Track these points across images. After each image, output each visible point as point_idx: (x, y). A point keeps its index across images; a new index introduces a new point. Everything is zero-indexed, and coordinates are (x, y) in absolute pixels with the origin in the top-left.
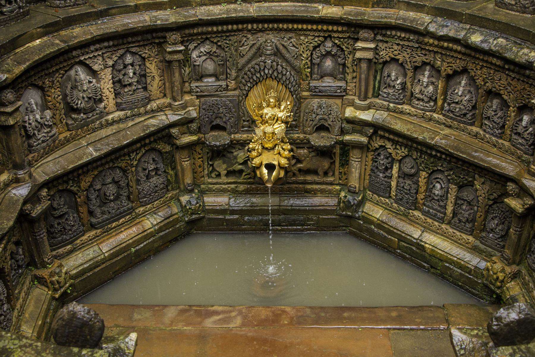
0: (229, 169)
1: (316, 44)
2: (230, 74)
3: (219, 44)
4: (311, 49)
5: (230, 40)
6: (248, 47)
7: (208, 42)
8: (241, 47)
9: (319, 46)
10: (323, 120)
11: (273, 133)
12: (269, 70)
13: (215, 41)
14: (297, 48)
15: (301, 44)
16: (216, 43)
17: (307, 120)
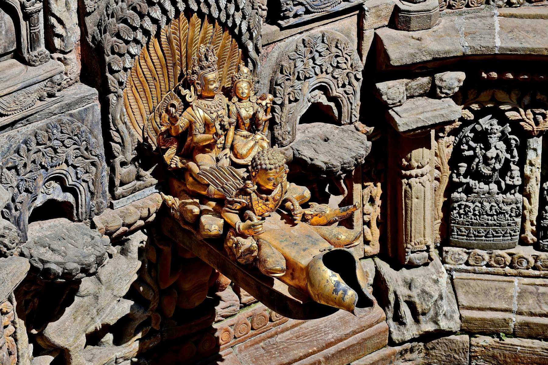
0: (91, 329)
2: (60, 36)
10: (317, 92)
17: (282, 105)
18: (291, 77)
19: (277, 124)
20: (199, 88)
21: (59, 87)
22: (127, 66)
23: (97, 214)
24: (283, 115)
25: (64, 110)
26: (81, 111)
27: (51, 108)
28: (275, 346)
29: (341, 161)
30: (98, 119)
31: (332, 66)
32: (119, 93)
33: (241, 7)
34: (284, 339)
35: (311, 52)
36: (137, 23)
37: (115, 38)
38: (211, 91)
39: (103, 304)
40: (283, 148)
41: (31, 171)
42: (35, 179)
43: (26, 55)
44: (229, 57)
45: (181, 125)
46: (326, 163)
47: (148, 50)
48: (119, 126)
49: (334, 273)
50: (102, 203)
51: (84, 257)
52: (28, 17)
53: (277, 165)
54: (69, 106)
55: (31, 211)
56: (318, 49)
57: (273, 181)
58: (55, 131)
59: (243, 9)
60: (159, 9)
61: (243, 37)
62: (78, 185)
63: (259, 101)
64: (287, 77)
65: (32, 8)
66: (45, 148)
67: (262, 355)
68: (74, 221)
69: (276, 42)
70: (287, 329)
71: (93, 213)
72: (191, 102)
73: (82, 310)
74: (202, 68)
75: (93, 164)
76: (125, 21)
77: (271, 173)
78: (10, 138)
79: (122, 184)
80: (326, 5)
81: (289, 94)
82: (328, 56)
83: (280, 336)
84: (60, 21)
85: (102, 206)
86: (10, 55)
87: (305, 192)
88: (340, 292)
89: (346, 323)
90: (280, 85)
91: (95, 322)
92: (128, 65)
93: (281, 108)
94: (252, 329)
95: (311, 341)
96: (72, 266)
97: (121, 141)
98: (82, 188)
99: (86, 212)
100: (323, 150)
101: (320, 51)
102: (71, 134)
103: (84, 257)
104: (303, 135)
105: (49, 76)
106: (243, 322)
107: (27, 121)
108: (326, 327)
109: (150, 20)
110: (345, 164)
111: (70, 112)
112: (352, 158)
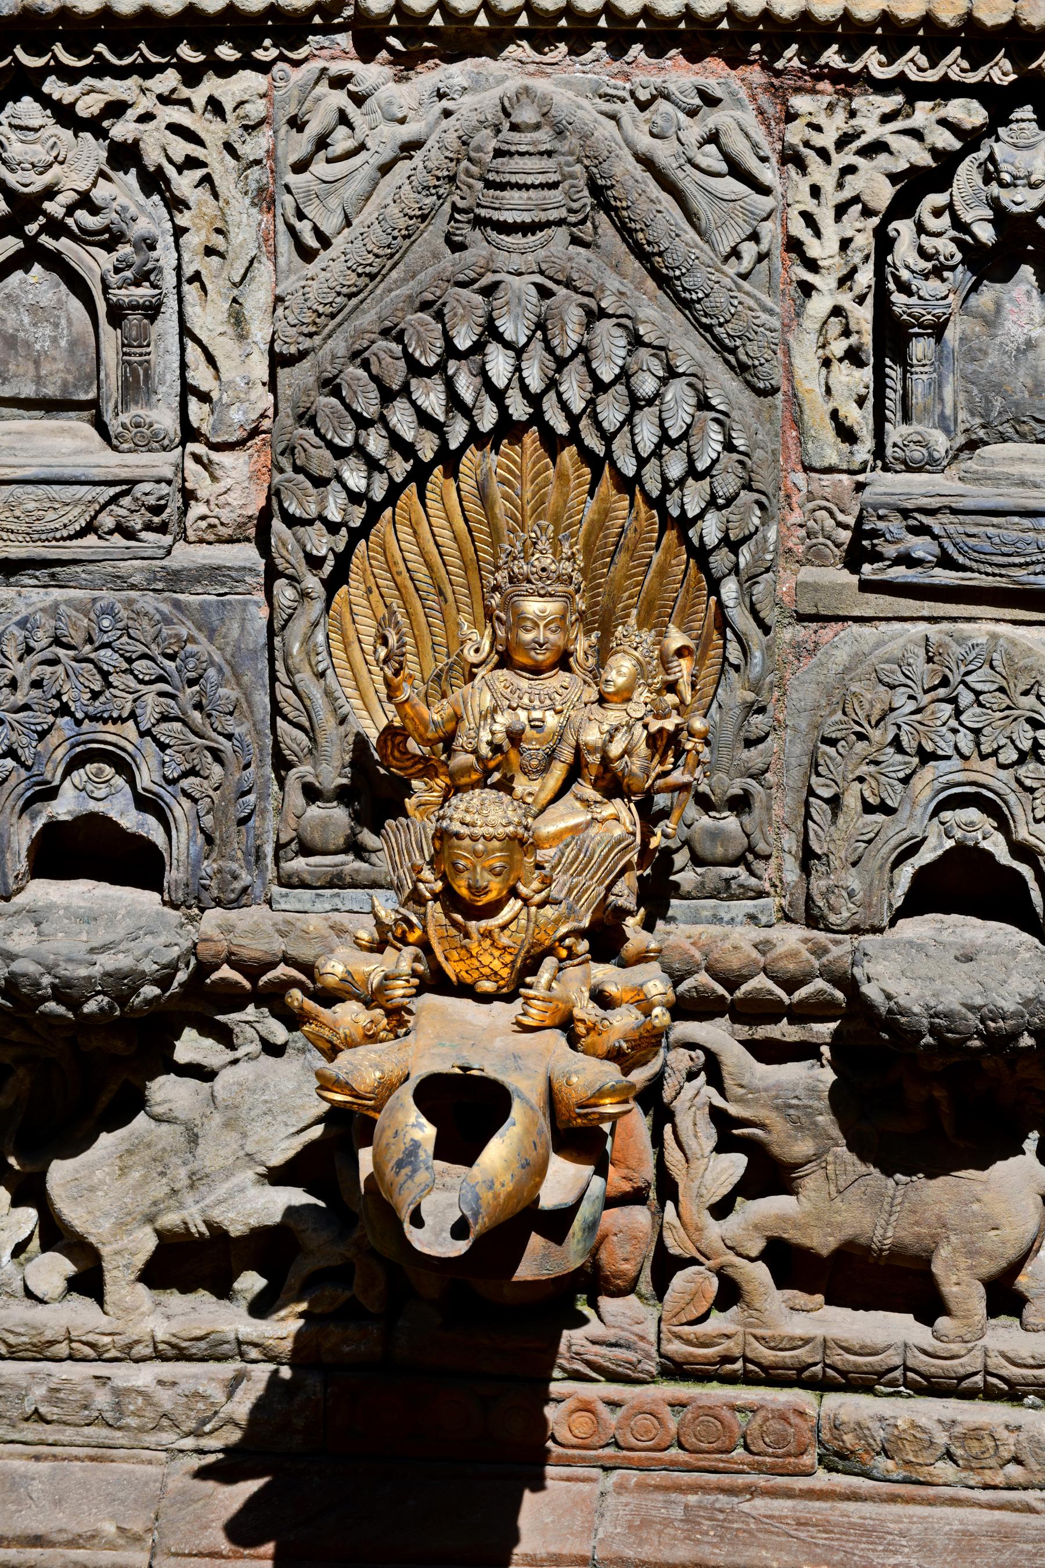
0: (170, 1220)
1: (912, 154)
2: (205, 397)
3: (122, 130)
4: (883, 194)
5: (215, 106)
6: (365, 164)
7: (27, 109)
8: (300, 167)
9: (939, 173)
10: (972, 814)
11: (520, 843)
12: (520, 352)
13: (88, 106)
14: (764, 190)
15: (792, 158)
16: (94, 126)
17: (835, 802)
18: (875, 735)
19: (818, 857)
20: (501, 633)
21: (156, 520)
22: (330, 517)
23: (219, 903)
24: (835, 836)
25: (160, 585)
26: (210, 604)
27: (122, 564)
28: (721, 1516)
29: (932, 1003)
30: (256, 642)
31: (1016, 748)
32: (303, 585)
33: (701, 466)
34: (762, 1512)
35: (945, 682)
36: (368, 404)
37: (309, 433)
38: (526, 648)
39: (207, 1163)
41: (26, 707)
42: (42, 735)
43: (108, 417)
45: (436, 717)
46: (889, 997)
47: (424, 506)
48: (298, 677)
49: (423, 1120)
50: (235, 877)
51: (70, 960)
52: (117, 315)
53: (478, 831)
54: (176, 580)
56: (968, 679)
57: (466, 874)
58: (106, 623)
59: (707, 472)
60: (442, 388)
61: (712, 559)
62: (168, 798)
63: (649, 719)
64: (858, 729)
65: (123, 291)
67: (667, 1522)
68: (165, 903)
69: (844, 619)
70: (788, 1494)
71: (205, 896)
72: (477, 666)
73: (147, 1154)
74: (512, 579)
75: (217, 755)
76: (331, 386)
77: (459, 848)
79: (306, 850)
80: (1011, 560)
81: (861, 779)
83: (758, 1502)
84: (211, 360)
85: (238, 885)
86: (86, 414)
87: (650, 984)
88: (407, 1170)
89: (972, 1550)
90: (832, 742)
91: (181, 1206)
92: (334, 515)
93: (835, 815)
94: (681, 1446)
95: (831, 1548)
96: (17, 966)
97: (307, 724)
98: (180, 810)
99: (187, 885)
100: (922, 972)
101: (979, 687)
102: (153, 646)
103: (70, 960)
104: (932, 933)
105: (124, 474)
106: (647, 1408)
107: (53, 576)
108: (902, 1535)
109: (412, 411)
110: (937, 1015)
112: (971, 1008)
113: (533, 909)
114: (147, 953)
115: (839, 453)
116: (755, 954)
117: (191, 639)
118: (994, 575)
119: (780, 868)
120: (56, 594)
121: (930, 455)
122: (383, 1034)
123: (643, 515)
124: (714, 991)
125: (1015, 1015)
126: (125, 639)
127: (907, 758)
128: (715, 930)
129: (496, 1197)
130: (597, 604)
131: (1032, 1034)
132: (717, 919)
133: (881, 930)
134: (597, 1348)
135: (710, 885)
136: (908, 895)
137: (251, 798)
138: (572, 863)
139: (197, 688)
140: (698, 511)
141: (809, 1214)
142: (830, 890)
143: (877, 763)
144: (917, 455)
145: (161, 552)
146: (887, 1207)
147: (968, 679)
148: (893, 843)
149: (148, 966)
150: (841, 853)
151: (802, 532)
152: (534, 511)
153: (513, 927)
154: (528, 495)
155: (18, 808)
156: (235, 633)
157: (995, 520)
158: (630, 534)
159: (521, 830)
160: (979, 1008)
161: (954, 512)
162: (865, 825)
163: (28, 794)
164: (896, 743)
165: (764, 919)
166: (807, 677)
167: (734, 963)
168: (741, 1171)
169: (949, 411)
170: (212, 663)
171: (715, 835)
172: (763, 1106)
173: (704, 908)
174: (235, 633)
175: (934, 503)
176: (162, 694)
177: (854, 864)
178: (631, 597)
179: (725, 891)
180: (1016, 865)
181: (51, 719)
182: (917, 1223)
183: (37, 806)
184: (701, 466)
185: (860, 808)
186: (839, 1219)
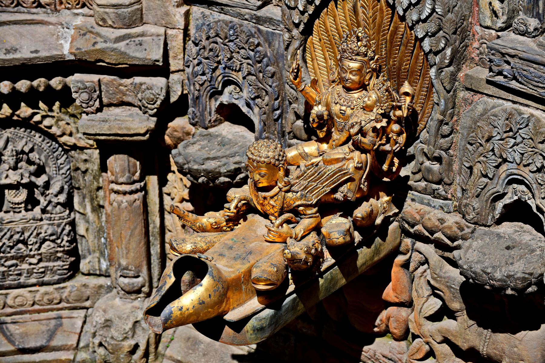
10: (523, 188)
25: (254, 21)
35: (511, 130)
40: (467, 223)
42: (214, 70)
44: (423, 74)
49: (172, 275)
53: (254, 158)
54: (259, 20)
55: (218, 103)
66: (222, 43)
69: (482, 93)
78: (204, 16)
82: (534, 149)
87: (333, 233)
90: (471, 144)
98: (256, 110)
101: (523, 135)
103: (194, 161)
107: (222, 9)
111: (261, 27)
113: (283, 193)
114: (224, 165)
115: (492, 21)
116: (437, 223)
117: (259, 45)
118: (533, 89)
119: (455, 190)
120: (223, 17)
121: (527, 30)
122: (225, 228)
123: (409, 32)
124: (424, 234)
125: (499, 280)
126: (238, 40)
127: (496, 159)
128: (427, 208)
129: (181, 314)
130: (395, 65)
131: (512, 289)
132: (429, 205)
133: (489, 226)
134: (384, 359)
135: (429, 191)
136: (501, 214)
137: (278, 112)
138: (310, 177)
139: (260, 65)
140: (422, 36)
141: (458, 332)
142: (466, 205)
143: (487, 158)
144: (521, 29)
145: (255, 8)
146: (484, 339)
147: (520, 131)
148: (491, 192)
149: (223, 170)
150: (473, 191)
151: (478, 52)
152: (373, 21)
153: (276, 198)
154: (371, 14)
155: (208, 96)
156: (277, 46)
157: (535, 66)
158: (404, 38)
159: (273, 161)
160: (489, 274)
161: (520, 58)
162: (481, 182)
163: (211, 91)
164: (493, 150)
165: (446, 210)
166: (467, 114)
167: (429, 225)
168: (439, 307)
169: (541, 12)
170: (265, 56)
171: (429, 170)
172: (443, 284)
173: (425, 199)
174: (277, 46)
175: (513, 52)
176: (248, 64)
177: (477, 196)
178: (406, 65)
179: (434, 194)
180: (538, 214)
181: (215, 65)
182: (494, 349)
183: (217, 96)
184: (423, 17)
185: (479, 174)
186: (468, 338)
